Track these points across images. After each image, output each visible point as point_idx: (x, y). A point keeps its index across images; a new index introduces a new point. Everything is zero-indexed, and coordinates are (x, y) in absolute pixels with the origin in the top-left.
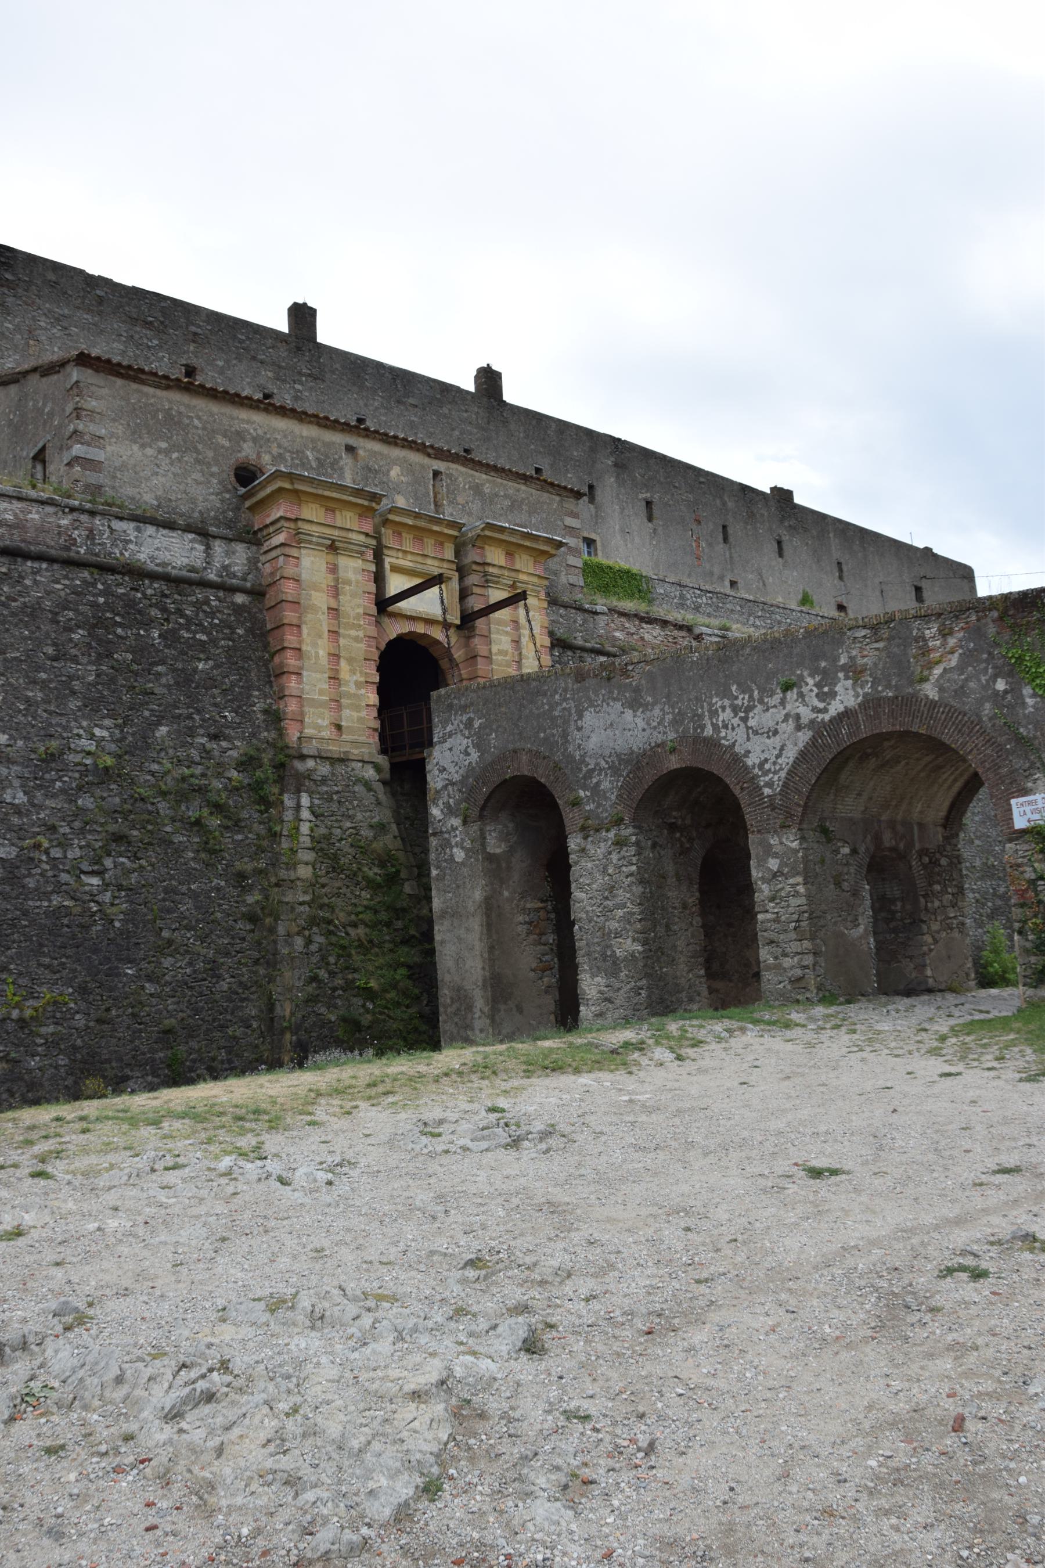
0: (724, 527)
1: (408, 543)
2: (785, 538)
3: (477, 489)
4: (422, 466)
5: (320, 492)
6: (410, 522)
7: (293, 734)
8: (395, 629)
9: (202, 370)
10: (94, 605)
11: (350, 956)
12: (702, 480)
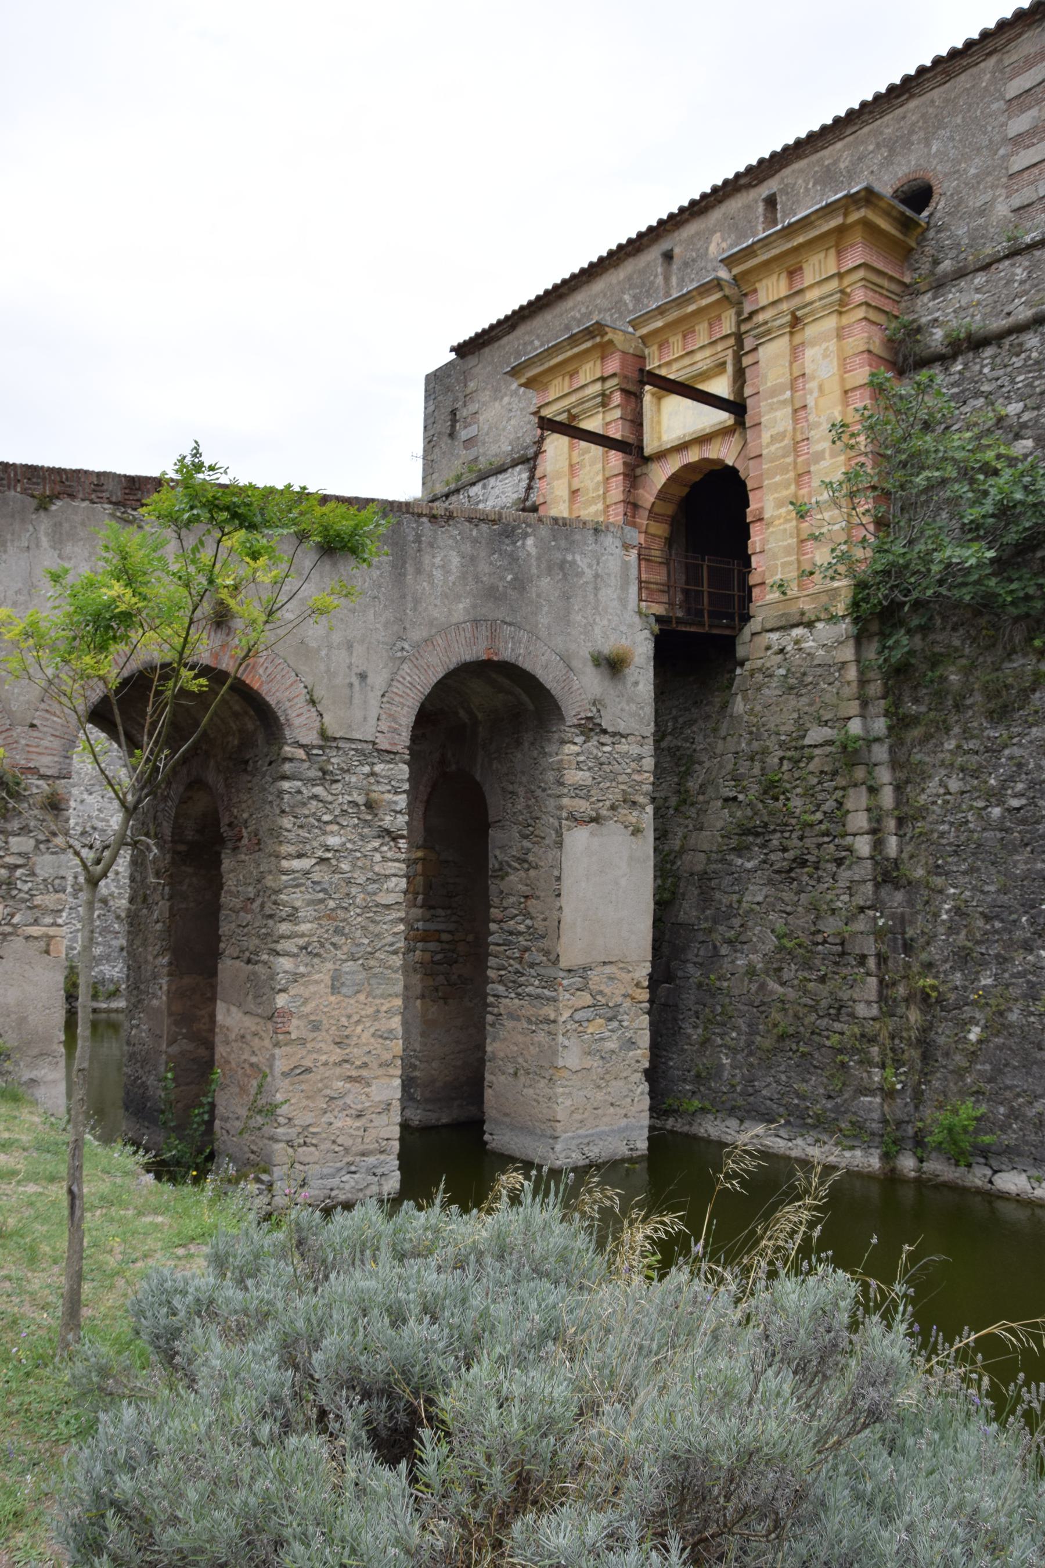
5: (546, 366)
6: (659, 324)
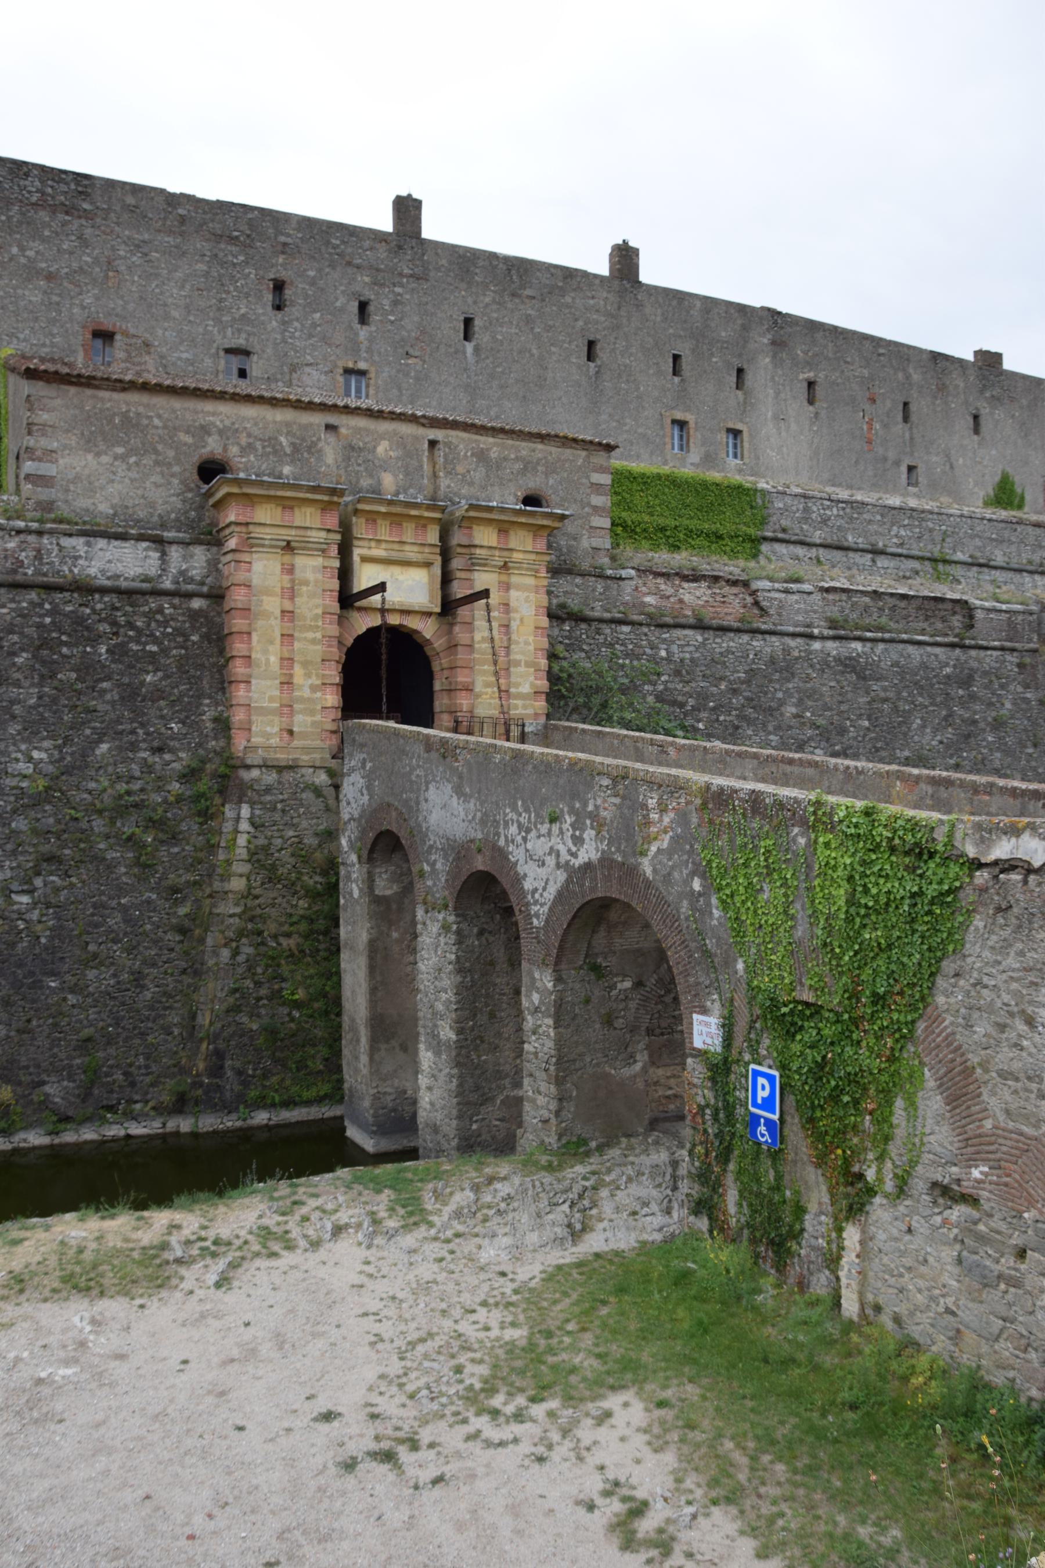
0: (906, 404)
1: (384, 531)
2: (985, 411)
3: (481, 456)
4: (416, 438)
6: (383, 509)
7: (239, 743)
8: (363, 623)
9: (292, 283)
10: (40, 626)
11: (279, 965)
12: (881, 351)
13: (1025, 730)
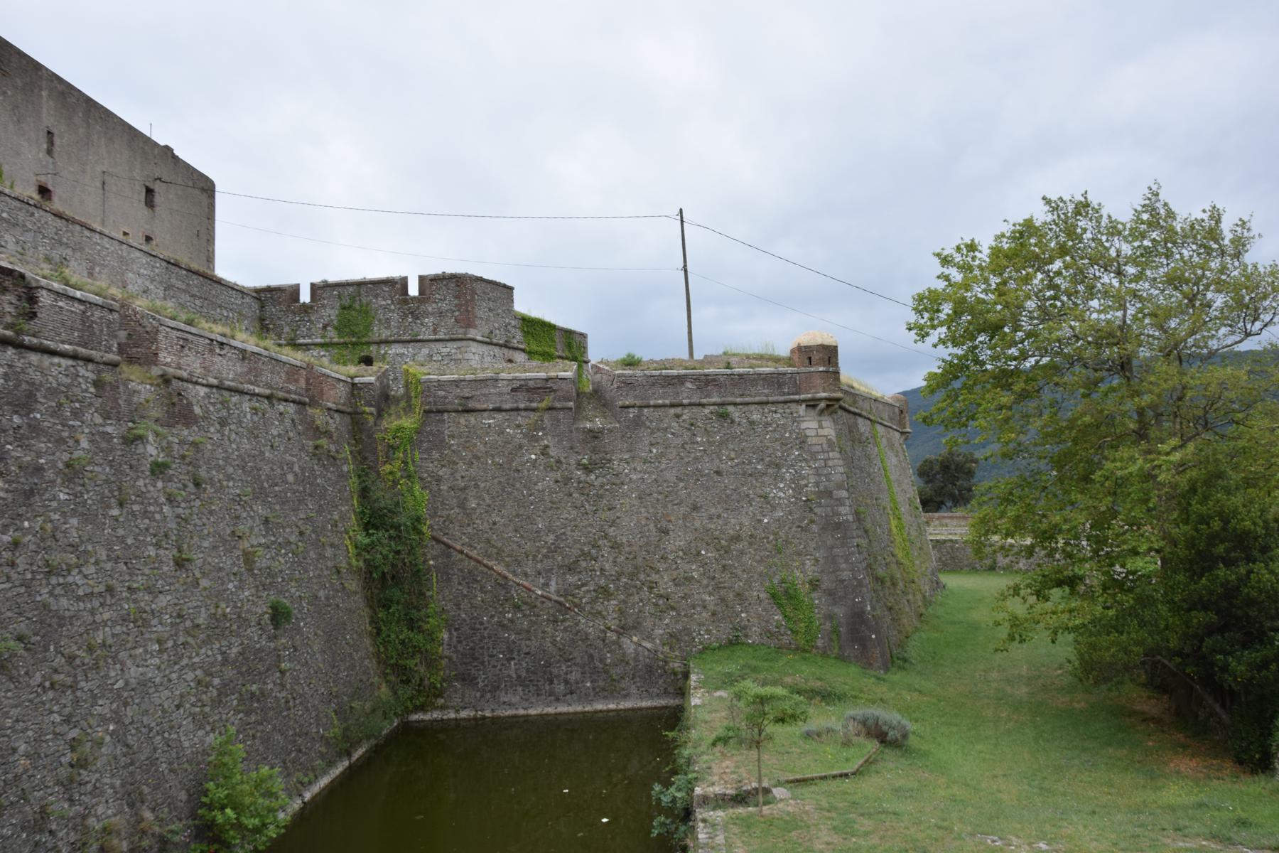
13: (107, 481)
